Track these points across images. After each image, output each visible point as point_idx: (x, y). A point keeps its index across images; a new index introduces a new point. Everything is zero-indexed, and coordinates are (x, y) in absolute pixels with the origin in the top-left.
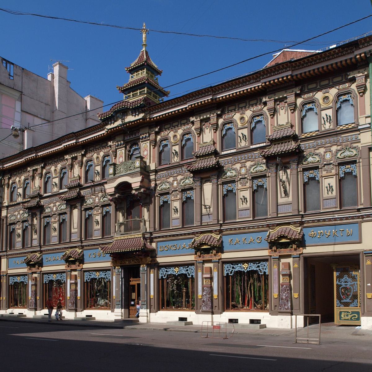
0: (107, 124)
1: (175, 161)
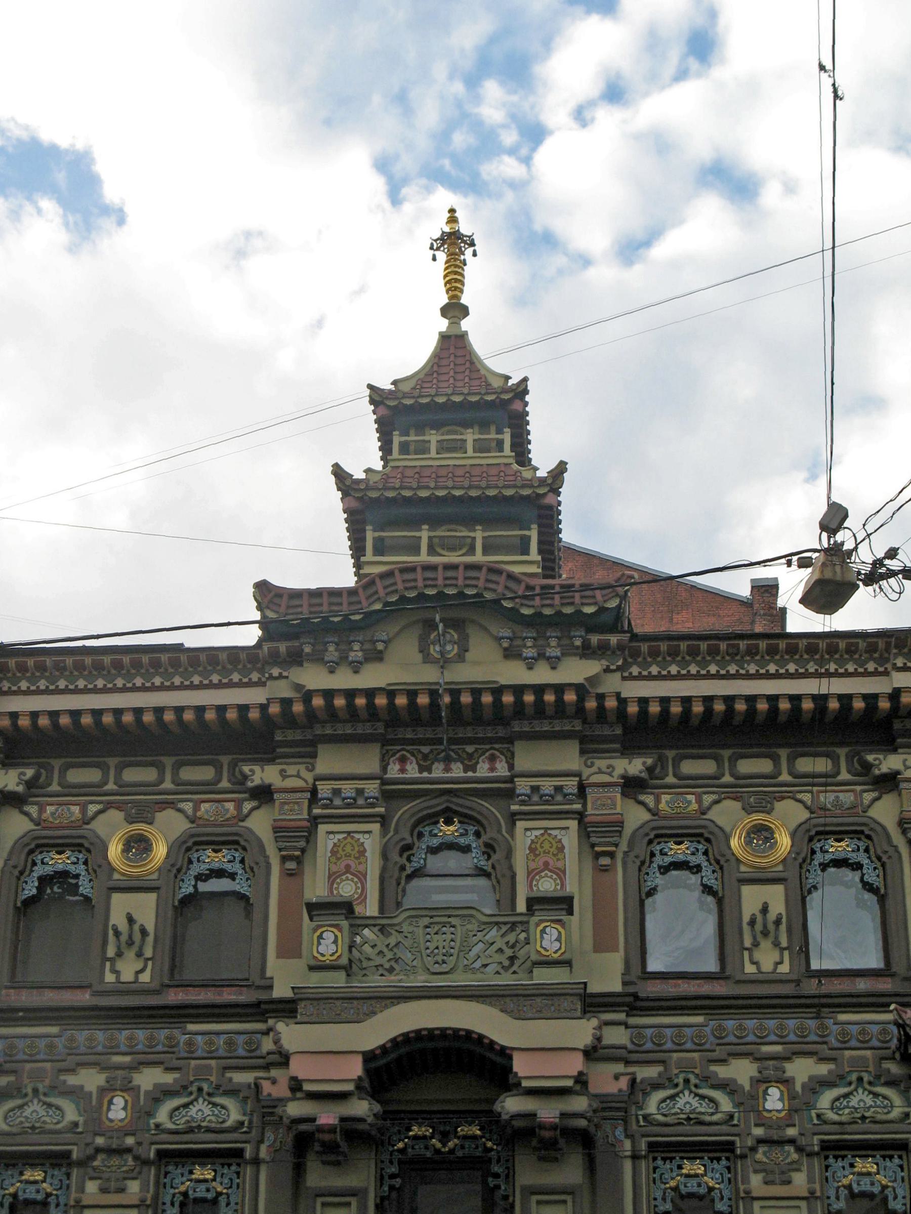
0: (296, 659)
1: (767, 966)
